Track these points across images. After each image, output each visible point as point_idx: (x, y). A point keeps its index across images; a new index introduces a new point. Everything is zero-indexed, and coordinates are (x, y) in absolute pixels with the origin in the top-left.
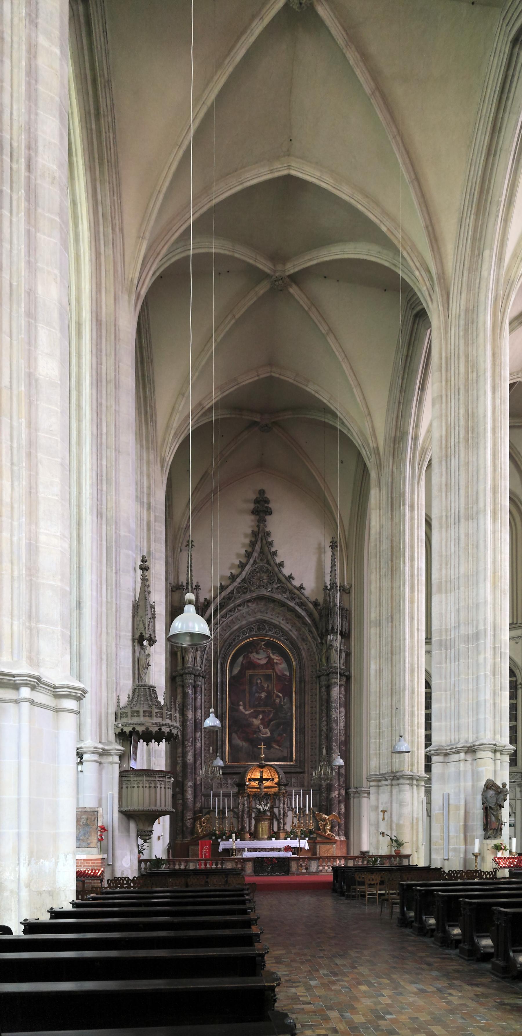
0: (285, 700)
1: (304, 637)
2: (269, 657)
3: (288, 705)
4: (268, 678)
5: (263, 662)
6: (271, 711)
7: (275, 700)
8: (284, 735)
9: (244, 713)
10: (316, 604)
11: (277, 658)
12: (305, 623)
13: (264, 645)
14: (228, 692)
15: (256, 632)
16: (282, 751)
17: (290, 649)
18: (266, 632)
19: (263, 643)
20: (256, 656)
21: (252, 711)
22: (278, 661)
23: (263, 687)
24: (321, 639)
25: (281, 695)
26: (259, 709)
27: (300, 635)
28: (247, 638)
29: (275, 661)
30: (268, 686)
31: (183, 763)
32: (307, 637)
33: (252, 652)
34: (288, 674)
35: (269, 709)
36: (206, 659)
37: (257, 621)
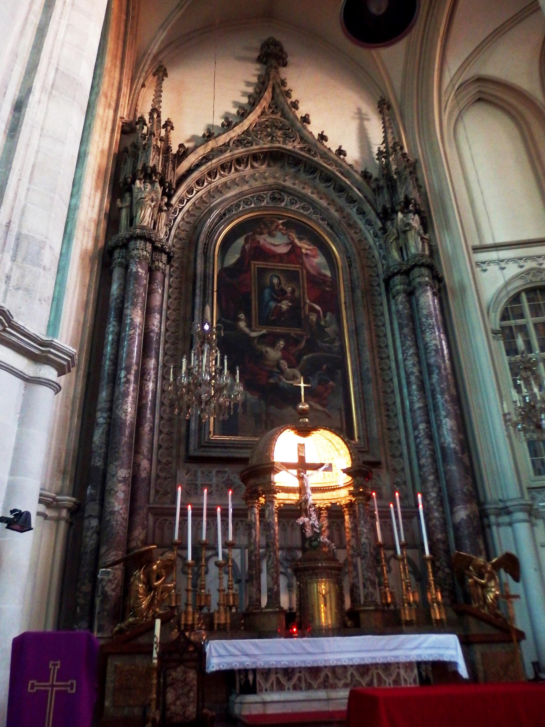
0: (327, 318)
1: (351, 222)
2: (292, 243)
3: (334, 327)
4: (293, 276)
5: (283, 250)
6: (302, 336)
7: (307, 317)
8: (331, 383)
9: (247, 335)
10: (366, 175)
11: (306, 246)
12: (352, 200)
13: (282, 224)
14: (215, 294)
15: (267, 203)
16: (329, 416)
17: (329, 235)
18: (286, 205)
19: (281, 222)
20: (270, 240)
21: (264, 331)
22: (308, 252)
23: (283, 292)
24: (384, 224)
25: (318, 308)
26: (278, 330)
27: (344, 217)
28: (252, 210)
29: (304, 251)
30: (293, 291)
31: (109, 424)
32: (355, 222)
33: (261, 234)
34: (328, 273)
35: (298, 331)
36: (175, 236)
37: (270, 188)
